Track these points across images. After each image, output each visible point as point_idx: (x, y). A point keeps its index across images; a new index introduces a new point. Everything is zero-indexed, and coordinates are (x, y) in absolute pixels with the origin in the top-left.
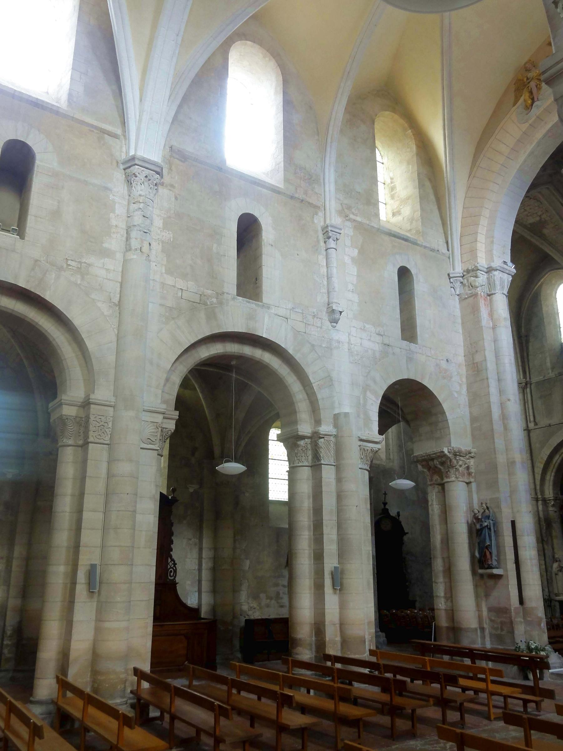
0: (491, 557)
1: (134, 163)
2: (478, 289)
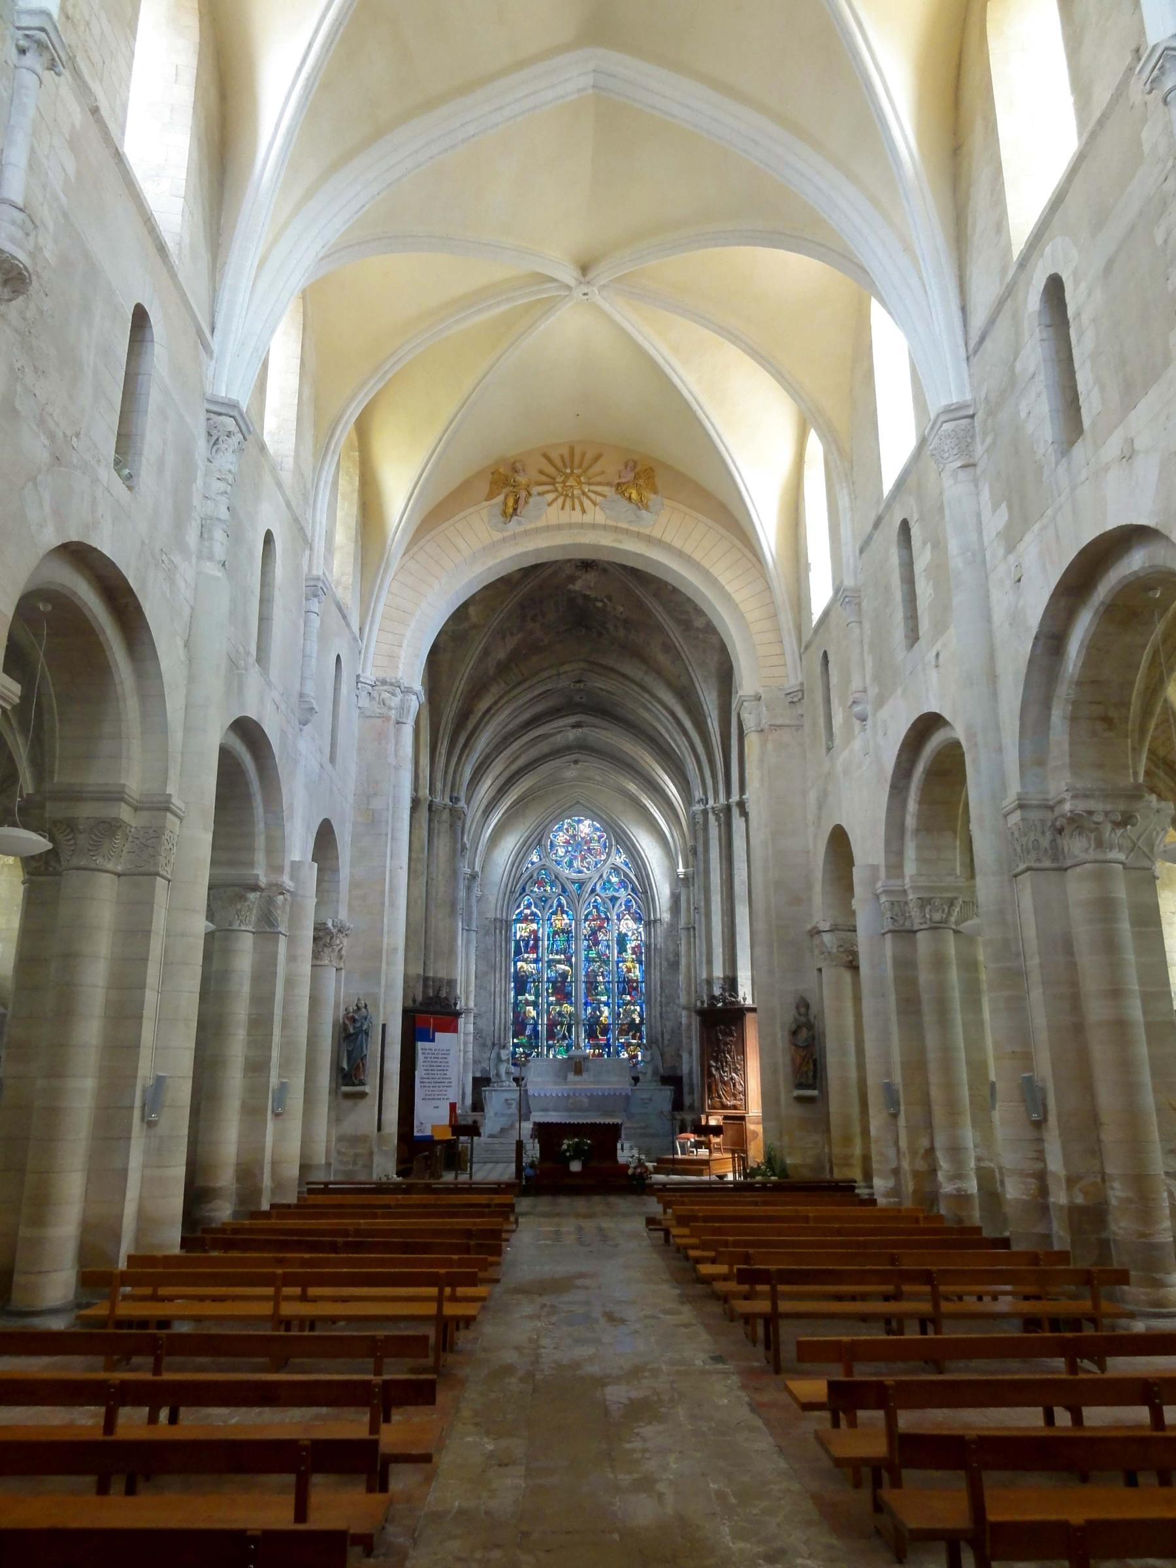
0: (364, 1071)
1: (232, 413)
2: (393, 711)
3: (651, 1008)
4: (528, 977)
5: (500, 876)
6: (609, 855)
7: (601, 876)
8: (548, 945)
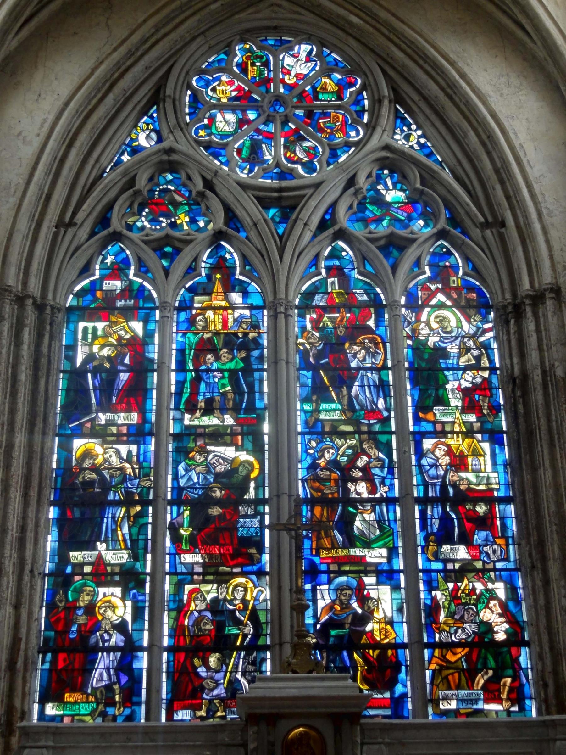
3: (547, 583)
4: (106, 486)
5: (25, 171)
6: (370, 128)
7: (351, 182)
8: (180, 384)
